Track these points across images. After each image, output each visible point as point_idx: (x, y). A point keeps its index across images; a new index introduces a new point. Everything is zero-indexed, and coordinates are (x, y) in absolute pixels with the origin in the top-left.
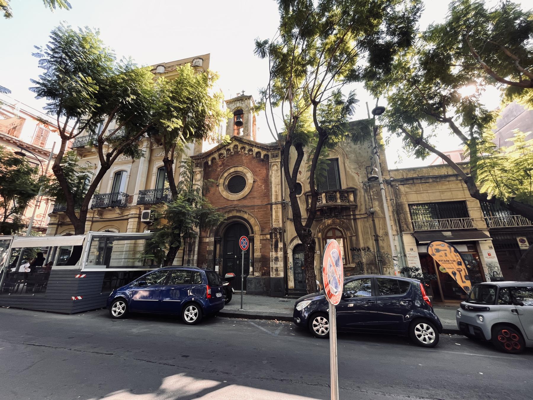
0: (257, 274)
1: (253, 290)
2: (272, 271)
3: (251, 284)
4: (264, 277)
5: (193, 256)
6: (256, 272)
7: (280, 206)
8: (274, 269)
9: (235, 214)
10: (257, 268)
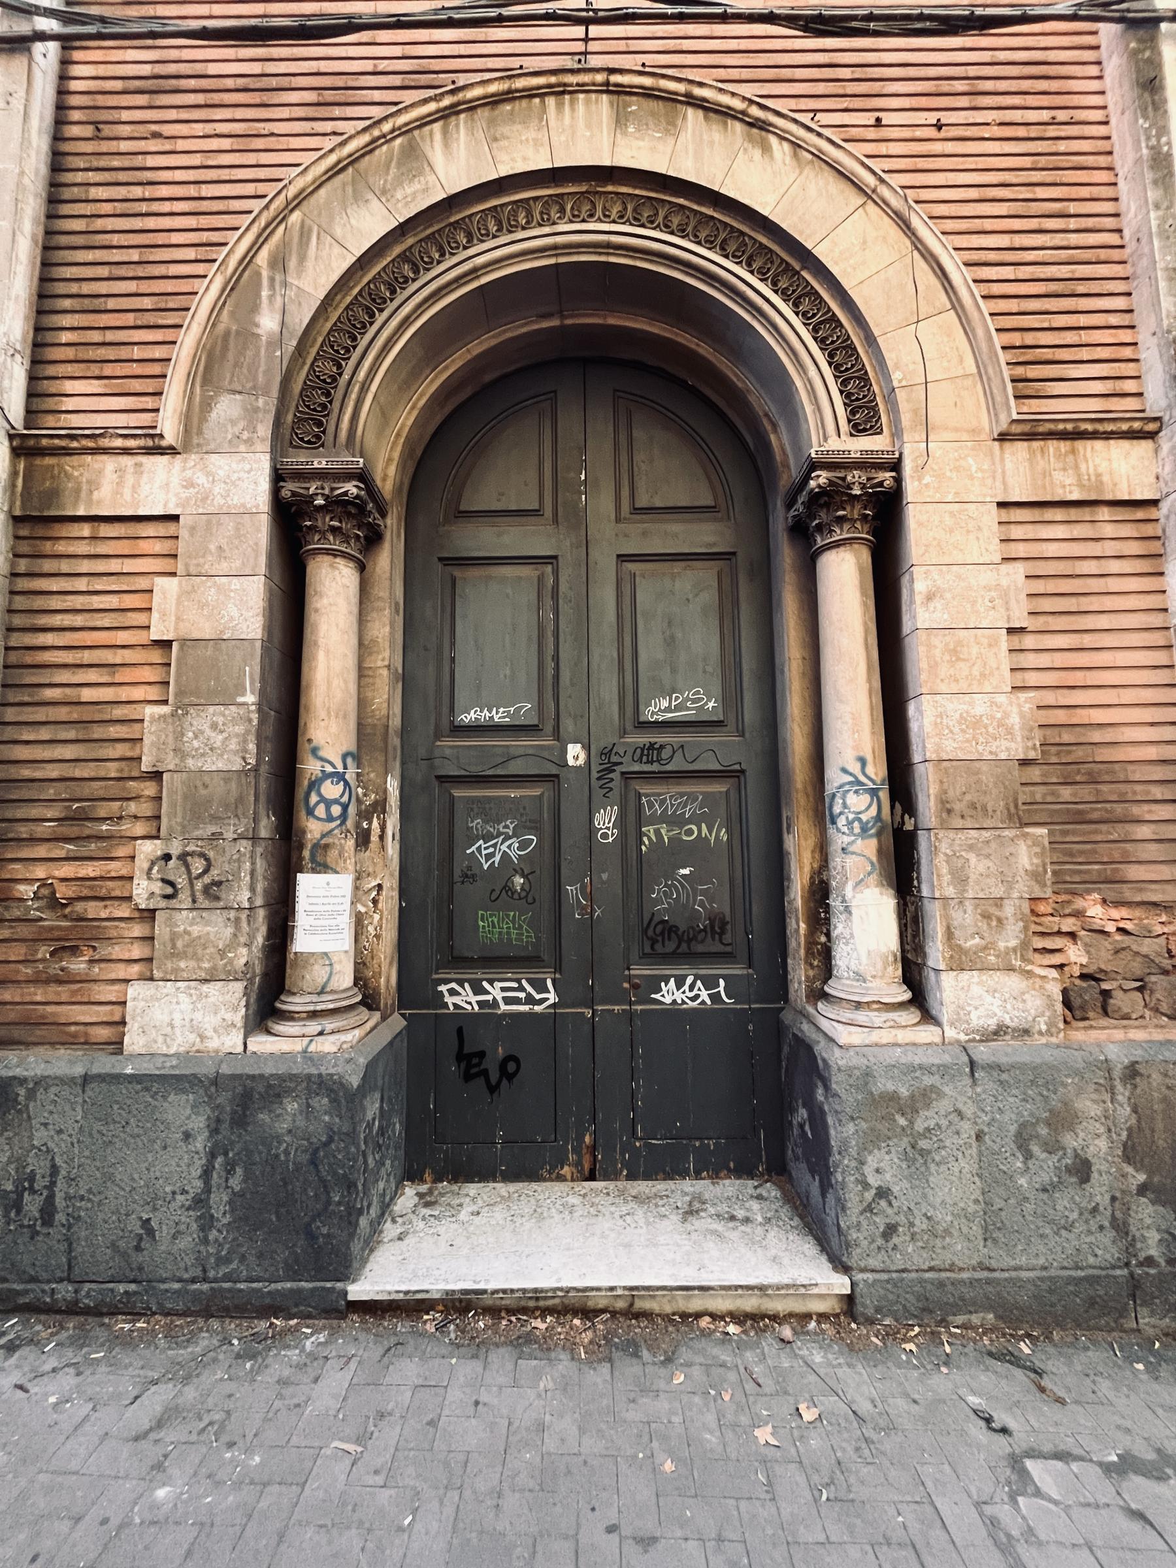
0: (985, 998)
1: (962, 1251)
3: (918, 1157)
4: (1110, 1041)
6: (961, 961)
9: (583, 135)
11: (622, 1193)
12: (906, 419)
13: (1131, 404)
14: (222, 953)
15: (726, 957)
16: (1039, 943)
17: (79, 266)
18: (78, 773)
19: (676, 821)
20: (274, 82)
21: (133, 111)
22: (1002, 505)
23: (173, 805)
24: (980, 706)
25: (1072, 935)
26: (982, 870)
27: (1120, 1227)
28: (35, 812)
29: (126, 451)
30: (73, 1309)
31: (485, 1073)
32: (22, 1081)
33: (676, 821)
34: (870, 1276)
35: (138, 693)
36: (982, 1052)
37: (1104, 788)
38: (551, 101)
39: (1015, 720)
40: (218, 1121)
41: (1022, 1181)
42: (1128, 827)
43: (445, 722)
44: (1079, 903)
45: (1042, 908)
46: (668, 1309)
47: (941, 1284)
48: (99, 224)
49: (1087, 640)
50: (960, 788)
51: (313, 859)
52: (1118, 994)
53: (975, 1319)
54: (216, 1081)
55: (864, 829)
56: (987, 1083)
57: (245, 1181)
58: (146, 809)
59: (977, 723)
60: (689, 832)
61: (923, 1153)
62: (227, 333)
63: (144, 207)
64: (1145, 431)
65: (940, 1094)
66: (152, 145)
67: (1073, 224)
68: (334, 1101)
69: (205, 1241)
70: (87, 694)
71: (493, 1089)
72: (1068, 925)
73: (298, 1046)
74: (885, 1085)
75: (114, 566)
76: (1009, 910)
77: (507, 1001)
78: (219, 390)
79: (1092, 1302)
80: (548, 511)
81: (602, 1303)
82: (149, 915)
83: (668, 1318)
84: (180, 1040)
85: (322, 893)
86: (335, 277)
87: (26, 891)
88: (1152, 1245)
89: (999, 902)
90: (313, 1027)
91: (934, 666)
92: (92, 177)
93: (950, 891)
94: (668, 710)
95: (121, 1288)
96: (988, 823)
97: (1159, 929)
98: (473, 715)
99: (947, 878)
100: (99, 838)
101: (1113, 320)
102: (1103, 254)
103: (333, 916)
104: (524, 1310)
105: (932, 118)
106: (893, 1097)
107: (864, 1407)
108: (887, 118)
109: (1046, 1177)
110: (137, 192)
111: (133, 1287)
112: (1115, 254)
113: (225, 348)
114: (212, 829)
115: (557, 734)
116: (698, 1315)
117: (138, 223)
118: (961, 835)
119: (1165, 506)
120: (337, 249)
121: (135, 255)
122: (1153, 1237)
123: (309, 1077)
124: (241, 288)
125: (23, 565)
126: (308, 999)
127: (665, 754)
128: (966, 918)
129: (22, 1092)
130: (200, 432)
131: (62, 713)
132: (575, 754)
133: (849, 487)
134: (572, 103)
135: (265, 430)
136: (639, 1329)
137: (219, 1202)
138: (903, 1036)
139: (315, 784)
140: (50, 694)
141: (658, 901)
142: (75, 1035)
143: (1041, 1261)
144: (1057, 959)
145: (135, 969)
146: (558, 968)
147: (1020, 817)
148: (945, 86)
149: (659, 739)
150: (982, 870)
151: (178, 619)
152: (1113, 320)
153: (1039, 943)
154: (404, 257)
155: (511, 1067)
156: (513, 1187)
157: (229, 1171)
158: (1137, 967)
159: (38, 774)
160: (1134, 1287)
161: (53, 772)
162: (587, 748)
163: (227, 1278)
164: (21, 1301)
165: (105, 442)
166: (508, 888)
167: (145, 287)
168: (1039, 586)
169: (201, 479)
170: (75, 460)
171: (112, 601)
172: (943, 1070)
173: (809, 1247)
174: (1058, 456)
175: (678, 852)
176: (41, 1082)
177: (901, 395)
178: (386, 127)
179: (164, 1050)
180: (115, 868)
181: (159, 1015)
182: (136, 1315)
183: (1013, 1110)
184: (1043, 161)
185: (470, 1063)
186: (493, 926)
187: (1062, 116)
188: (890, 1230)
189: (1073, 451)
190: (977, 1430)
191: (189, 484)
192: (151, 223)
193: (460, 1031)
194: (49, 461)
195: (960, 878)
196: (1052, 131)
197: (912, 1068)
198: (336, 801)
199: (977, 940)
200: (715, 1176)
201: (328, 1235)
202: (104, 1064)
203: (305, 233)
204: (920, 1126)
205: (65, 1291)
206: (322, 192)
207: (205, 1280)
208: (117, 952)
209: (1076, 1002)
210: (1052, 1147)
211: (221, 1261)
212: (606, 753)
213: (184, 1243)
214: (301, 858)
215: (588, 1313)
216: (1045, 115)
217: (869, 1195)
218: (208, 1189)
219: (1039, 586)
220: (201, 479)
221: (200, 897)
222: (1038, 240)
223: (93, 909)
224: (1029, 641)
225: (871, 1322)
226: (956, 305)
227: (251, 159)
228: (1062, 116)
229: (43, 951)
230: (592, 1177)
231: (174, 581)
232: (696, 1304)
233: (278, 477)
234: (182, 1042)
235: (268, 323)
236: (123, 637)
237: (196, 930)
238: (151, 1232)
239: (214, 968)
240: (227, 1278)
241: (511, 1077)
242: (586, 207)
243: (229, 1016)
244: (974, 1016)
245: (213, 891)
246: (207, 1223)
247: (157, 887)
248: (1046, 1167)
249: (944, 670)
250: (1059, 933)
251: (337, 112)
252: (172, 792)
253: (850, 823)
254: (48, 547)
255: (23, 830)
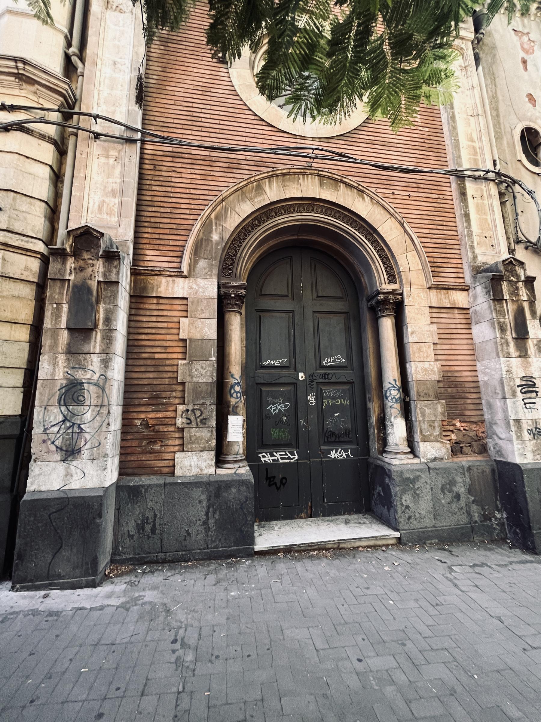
0: (431, 450)
1: (428, 522)
2: (520, 438)
3: (416, 496)
4: (464, 461)
5: (106, 363)
6: (425, 439)
7: (493, 189)
8: (525, 427)
9: (310, 188)
10: (431, 426)
11: (323, 520)
12: (404, 281)
13: (461, 280)
14: (207, 442)
15: (349, 442)
16: (444, 433)
17: (148, 212)
18: (155, 382)
19: (334, 398)
20: (214, 159)
21: (167, 163)
22: (430, 307)
23: (189, 393)
24: (427, 365)
25: (452, 431)
26: (429, 412)
27: (468, 513)
28: (140, 395)
29: (170, 276)
30: (164, 562)
31: (275, 483)
32: (143, 486)
33: (334, 398)
34: (405, 532)
35: (175, 356)
36: (431, 465)
37: (459, 389)
38: (301, 176)
39: (436, 369)
40: (210, 496)
41: (443, 501)
42: (466, 400)
43: (258, 365)
44: (454, 422)
45: (445, 423)
46: (349, 546)
47: (423, 532)
48: (156, 199)
49: (453, 347)
50: (422, 389)
51: (233, 411)
52: (465, 448)
53: (433, 541)
54: (209, 483)
55: (396, 400)
56: (433, 473)
57: (220, 515)
58: (179, 394)
59: (426, 370)
60: (338, 402)
61: (418, 495)
62: (202, 239)
63: (171, 195)
64: (465, 289)
65: (421, 477)
66: (174, 174)
67: (445, 228)
68: (248, 488)
69: (207, 536)
70: (157, 356)
71: (278, 489)
72: (451, 428)
73: (232, 471)
74: (407, 475)
75: (165, 313)
76: (436, 424)
77: (282, 459)
78: (200, 258)
79: (462, 534)
80: (290, 295)
81: (330, 546)
82: (182, 430)
83: (350, 549)
84: (193, 471)
85: (236, 422)
86: (236, 224)
87: (138, 422)
88: (476, 517)
89: (433, 422)
90: (237, 465)
91: (414, 353)
92: (153, 183)
93: (421, 419)
94: (330, 362)
95: (180, 553)
96: (430, 399)
97: (474, 429)
98: (268, 363)
99: (420, 415)
100: (163, 404)
101: (456, 256)
102: (453, 237)
103: (236, 428)
104: (308, 550)
105: (407, 193)
106: (408, 479)
107: (410, 561)
108: (396, 192)
109: (449, 500)
110: (169, 189)
111: (184, 553)
112: (456, 238)
113: (201, 244)
114: (203, 401)
115: (295, 369)
116: (358, 547)
117: (169, 200)
118: (423, 402)
119: (471, 310)
120: (237, 215)
121: (169, 210)
122: (476, 515)
123: (239, 480)
124: (207, 226)
125: (133, 312)
126: (233, 456)
127: (330, 376)
128: (425, 426)
129: (143, 490)
130: (194, 271)
131: (149, 362)
132: (301, 376)
133: (389, 299)
134: (307, 178)
135: (215, 271)
136: (343, 552)
137: (211, 522)
138: (410, 461)
139: (232, 387)
140: (144, 355)
141: (329, 424)
142: (157, 471)
143: (449, 524)
144: (448, 438)
145: (177, 448)
146: (298, 447)
147: (438, 397)
148: (411, 185)
149: (328, 371)
150: (429, 412)
151: (189, 332)
152: (456, 256)
153: (444, 433)
154: (255, 218)
155: (284, 481)
156: (287, 521)
157: (215, 513)
158: (469, 440)
159: (141, 383)
160: (472, 528)
161: (146, 382)
162: (305, 374)
163: (215, 547)
164: (146, 560)
165: (163, 273)
166: (281, 421)
167: (173, 221)
168: (441, 331)
169: (195, 286)
170: (152, 278)
171: (165, 325)
172: (421, 470)
173: (385, 527)
174: (444, 294)
175: (334, 408)
176: (150, 486)
177: (403, 274)
178: (252, 179)
179: (189, 474)
180: (169, 414)
181: (187, 463)
182: (186, 561)
183: (440, 481)
184: (437, 209)
185: (270, 480)
186: (275, 434)
187: (441, 197)
188: (410, 518)
189: (448, 293)
190: (439, 563)
191: (191, 288)
192: (174, 200)
193: (267, 469)
194: (142, 277)
195: (423, 415)
196: (439, 201)
197: (413, 470)
198: (239, 392)
199: (428, 433)
200: (350, 514)
201: (247, 531)
202: (169, 480)
203: (226, 210)
204: (416, 487)
205: (161, 556)
206: (232, 197)
207: (208, 548)
208: (170, 442)
209: (454, 450)
210: (450, 491)
211: (213, 542)
212: (311, 376)
213: (199, 537)
214: (229, 411)
215: (327, 550)
216: (437, 196)
217: (403, 508)
218: (208, 519)
219: (441, 331)
220: (195, 286)
221: (199, 424)
222: (437, 232)
223: (161, 428)
224: (439, 347)
225: (406, 545)
226: (416, 249)
227: (207, 183)
228: (441, 197)
229: (144, 443)
230: (311, 517)
231: (187, 319)
232: (357, 544)
233: (219, 287)
234: (195, 471)
235: (215, 237)
236: (169, 337)
237: (198, 434)
238: (189, 534)
239: (205, 447)
240: (215, 547)
241: (284, 484)
242: (311, 209)
243: (210, 462)
244: (428, 455)
245: (204, 422)
246: (208, 529)
247: (185, 420)
248: (449, 496)
249: (417, 355)
250: (449, 431)
251: (234, 171)
252: (189, 389)
253: (392, 399)
254: (142, 306)
255: (136, 402)
